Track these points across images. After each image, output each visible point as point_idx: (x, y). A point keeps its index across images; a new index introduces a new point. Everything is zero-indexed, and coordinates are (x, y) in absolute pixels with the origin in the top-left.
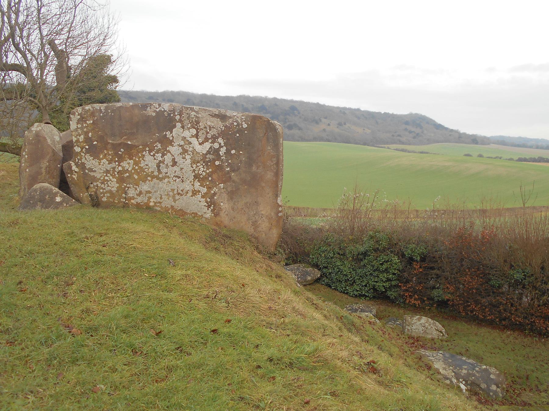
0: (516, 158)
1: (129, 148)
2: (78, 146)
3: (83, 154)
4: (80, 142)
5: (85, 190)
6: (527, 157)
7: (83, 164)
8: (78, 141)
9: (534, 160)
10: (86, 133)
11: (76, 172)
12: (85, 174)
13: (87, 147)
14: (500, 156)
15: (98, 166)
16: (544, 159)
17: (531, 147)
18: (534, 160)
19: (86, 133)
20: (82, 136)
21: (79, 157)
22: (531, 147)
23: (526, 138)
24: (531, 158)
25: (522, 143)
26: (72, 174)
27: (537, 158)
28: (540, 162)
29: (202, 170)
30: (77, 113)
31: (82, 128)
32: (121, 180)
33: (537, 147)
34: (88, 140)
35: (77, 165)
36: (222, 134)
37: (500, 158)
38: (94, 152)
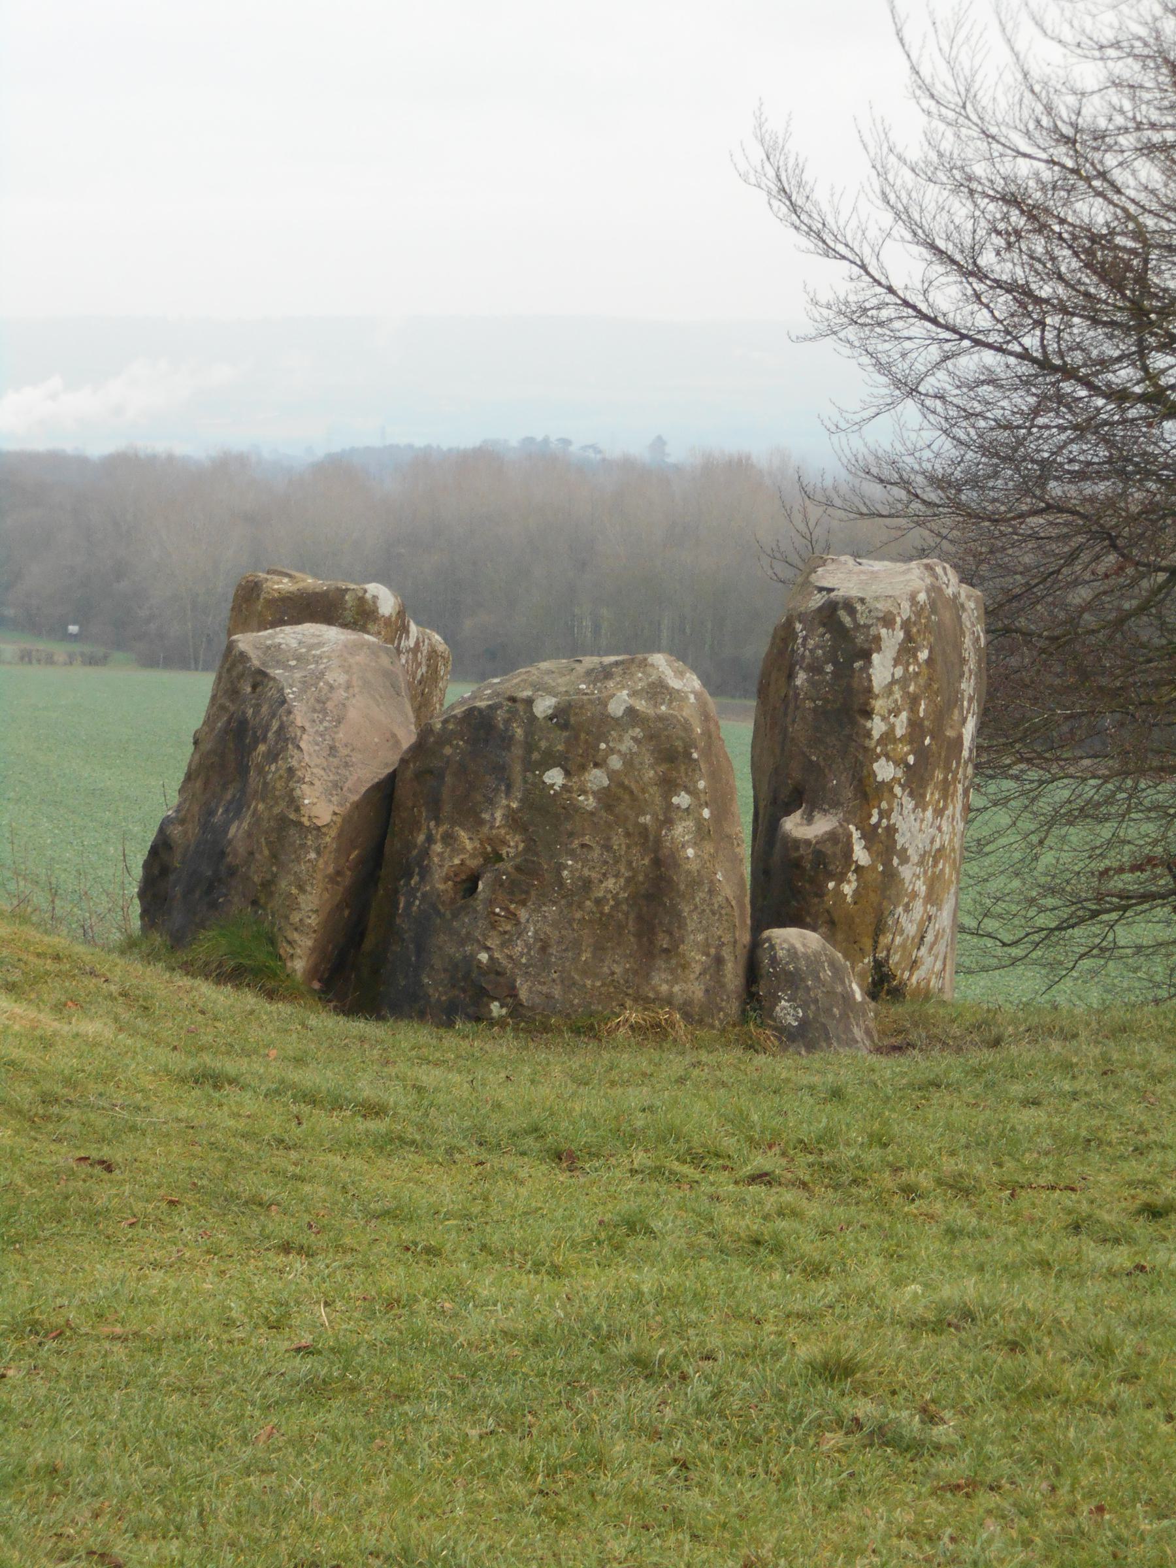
2: (888, 758)
3: (898, 790)
4: (895, 741)
5: (867, 943)
7: (891, 830)
8: (888, 737)
10: (914, 701)
11: (859, 869)
12: (890, 875)
13: (911, 759)
19: (914, 701)
20: (904, 715)
21: (884, 805)
26: (841, 878)
30: (898, 619)
31: (903, 682)
35: (870, 835)
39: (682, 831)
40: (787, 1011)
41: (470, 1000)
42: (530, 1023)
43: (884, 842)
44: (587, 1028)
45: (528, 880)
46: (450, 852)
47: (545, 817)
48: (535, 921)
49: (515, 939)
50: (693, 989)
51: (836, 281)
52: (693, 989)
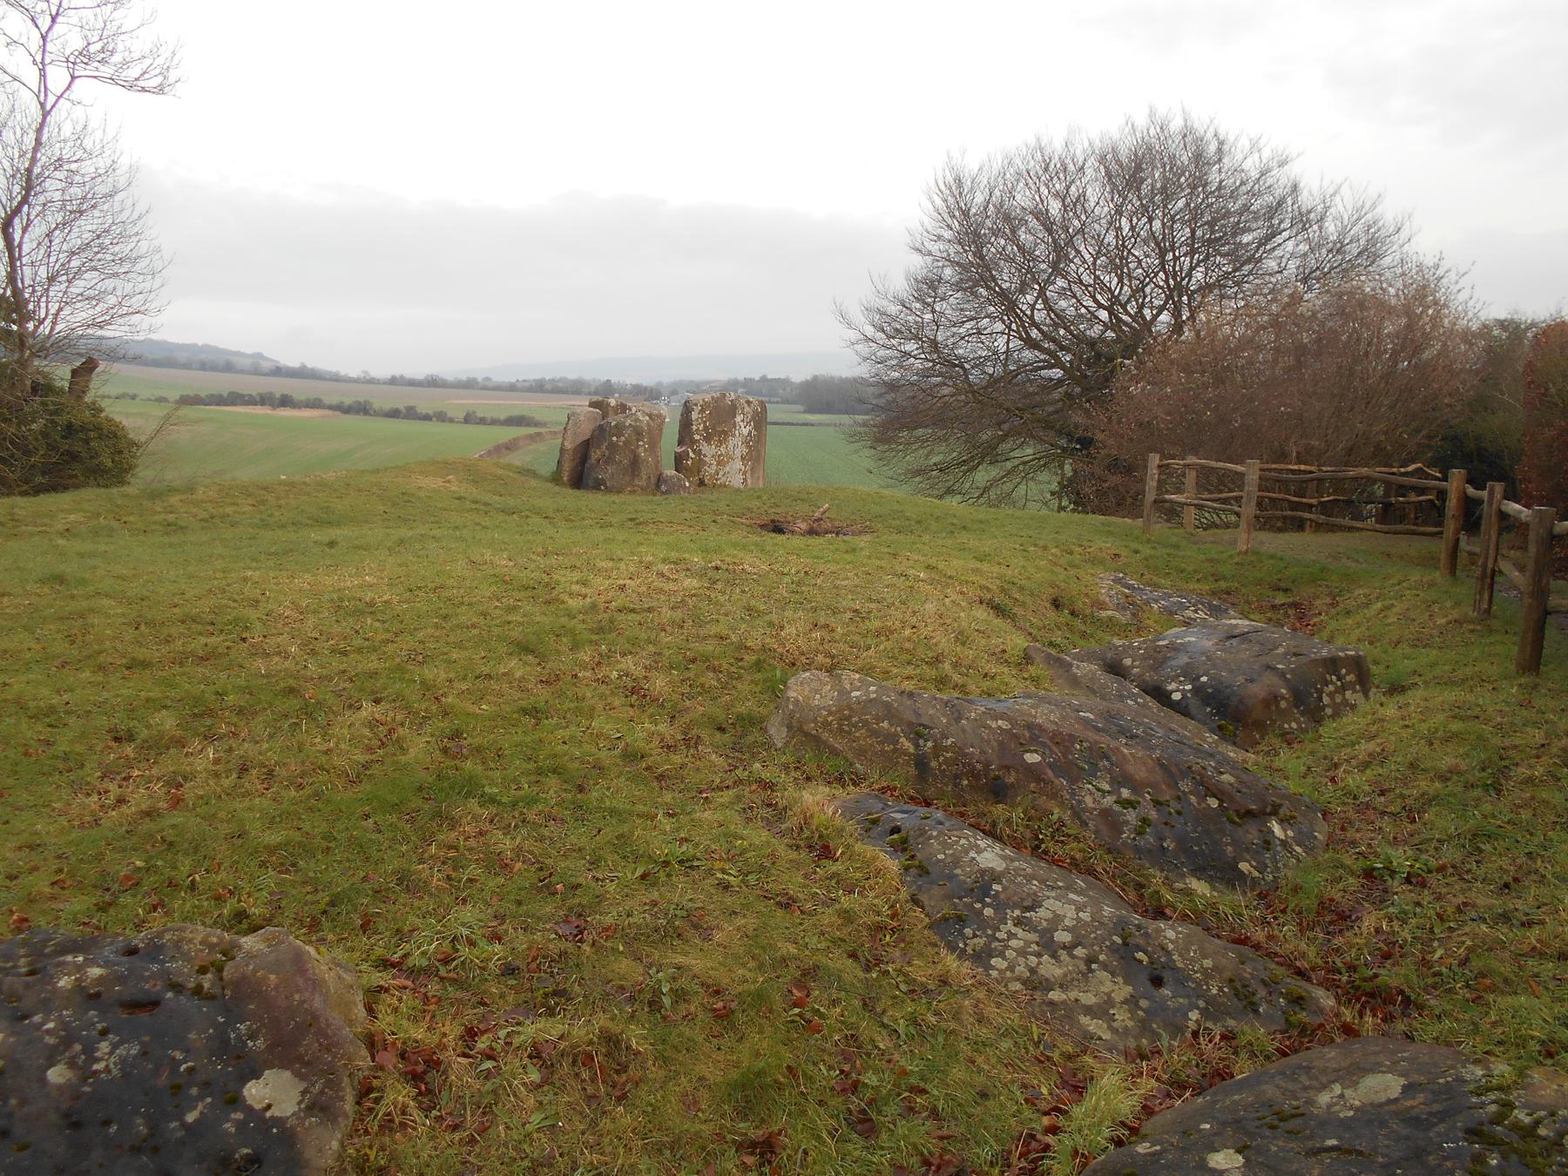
0: (174, 395)
1: (725, 433)
6: (203, 394)
9: (220, 401)
14: (131, 391)
15: (708, 450)
16: (242, 396)
17: (187, 366)
18: (220, 401)
22: (187, 366)
23: (166, 342)
24: (213, 396)
25: (222, 363)
27: (225, 394)
28: (233, 404)
29: (745, 450)
32: (719, 463)
33: (203, 366)
34: (706, 428)
36: (753, 418)
37: (133, 397)
38: (708, 439)
39: (641, 450)
40: (663, 488)
41: (597, 486)
42: (609, 490)
43: (698, 453)
44: (619, 492)
45: (609, 461)
46: (595, 454)
47: (613, 447)
48: (610, 469)
49: (606, 473)
50: (643, 483)
51: (853, 335)
52: (643, 483)
